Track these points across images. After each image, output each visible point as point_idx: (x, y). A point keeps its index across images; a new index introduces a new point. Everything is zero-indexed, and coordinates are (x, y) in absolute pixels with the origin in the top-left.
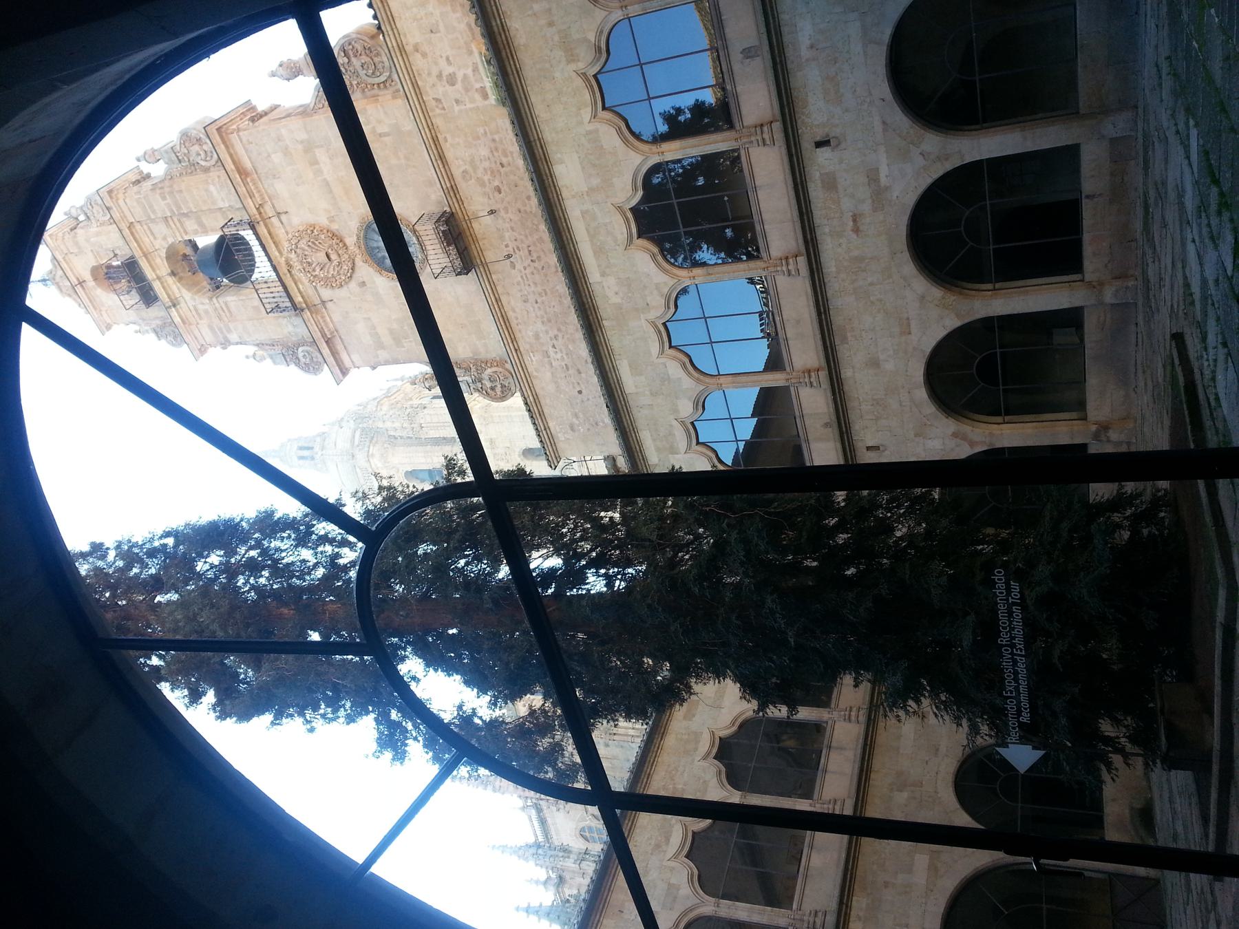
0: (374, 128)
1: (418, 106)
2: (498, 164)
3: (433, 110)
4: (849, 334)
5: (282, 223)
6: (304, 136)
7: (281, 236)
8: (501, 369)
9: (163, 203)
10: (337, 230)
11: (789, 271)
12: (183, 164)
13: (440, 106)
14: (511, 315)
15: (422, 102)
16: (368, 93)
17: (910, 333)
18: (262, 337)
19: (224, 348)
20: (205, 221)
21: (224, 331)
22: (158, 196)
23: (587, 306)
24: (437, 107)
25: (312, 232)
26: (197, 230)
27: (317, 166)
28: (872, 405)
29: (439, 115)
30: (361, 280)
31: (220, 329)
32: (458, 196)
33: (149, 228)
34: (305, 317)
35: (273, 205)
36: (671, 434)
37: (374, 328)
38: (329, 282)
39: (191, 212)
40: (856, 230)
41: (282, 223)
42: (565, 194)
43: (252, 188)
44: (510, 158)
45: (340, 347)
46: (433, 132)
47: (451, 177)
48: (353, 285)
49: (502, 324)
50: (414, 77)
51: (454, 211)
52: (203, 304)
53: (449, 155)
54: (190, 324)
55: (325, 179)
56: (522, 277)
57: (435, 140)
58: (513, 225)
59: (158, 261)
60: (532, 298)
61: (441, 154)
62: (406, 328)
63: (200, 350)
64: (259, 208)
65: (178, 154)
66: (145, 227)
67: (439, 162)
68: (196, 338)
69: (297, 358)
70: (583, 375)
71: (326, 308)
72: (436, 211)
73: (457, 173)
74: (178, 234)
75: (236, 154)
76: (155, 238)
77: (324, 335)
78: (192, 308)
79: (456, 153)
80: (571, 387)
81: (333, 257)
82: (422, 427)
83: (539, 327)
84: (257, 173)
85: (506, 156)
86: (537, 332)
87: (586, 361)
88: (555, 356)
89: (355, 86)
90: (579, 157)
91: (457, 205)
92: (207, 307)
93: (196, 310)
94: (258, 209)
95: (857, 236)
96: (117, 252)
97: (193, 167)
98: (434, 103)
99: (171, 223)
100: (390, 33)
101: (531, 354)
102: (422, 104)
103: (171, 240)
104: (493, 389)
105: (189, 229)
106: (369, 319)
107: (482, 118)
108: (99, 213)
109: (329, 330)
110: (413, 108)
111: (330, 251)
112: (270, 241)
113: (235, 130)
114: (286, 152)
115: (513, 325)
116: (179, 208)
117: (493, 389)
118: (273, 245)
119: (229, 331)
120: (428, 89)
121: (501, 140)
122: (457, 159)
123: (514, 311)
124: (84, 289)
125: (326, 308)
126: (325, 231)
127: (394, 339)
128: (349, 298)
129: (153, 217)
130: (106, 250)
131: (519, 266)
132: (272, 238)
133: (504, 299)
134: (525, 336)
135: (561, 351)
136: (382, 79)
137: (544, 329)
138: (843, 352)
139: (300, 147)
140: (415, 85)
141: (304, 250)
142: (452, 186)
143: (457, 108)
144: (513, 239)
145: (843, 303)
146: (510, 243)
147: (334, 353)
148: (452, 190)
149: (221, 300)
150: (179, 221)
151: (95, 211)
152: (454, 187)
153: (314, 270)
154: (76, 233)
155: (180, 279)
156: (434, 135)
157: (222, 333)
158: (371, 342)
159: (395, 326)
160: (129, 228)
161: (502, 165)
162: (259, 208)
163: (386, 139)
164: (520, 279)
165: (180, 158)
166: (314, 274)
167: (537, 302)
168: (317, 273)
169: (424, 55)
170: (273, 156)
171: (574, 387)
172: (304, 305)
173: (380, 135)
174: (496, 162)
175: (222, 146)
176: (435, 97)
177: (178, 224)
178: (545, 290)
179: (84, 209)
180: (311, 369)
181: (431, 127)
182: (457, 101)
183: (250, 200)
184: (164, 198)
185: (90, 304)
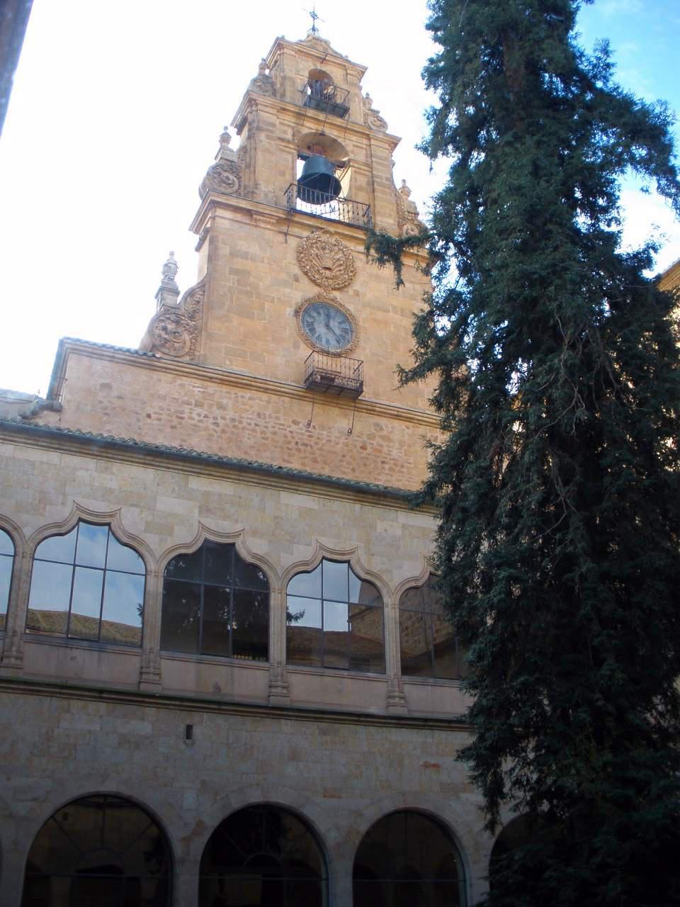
4: (329, 738)
8: (187, 350)
10: (347, 292)
11: (394, 697)
14: (248, 394)
17: (325, 796)
23: (382, 499)
25: (352, 272)
28: (246, 744)
36: (226, 517)
40: (426, 765)
44: (387, 472)
45: (239, 217)
46: (417, 422)
47: (381, 414)
48: (296, 270)
51: (357, 401)
53: (396, 423)
55: (389, 312)
56: (283, 425)
57: (409, 420)
58: (333, 444)
60: (261, 422)
62: (248, 288)
66: (364, 146)
68: (267, 106)
71: (280, 232)
73: (383, 421)
80: (157, 410)
83: (230, 414)
85: (390, 469)
87: (185, 441)
88: (195, 413)
91: (360, 406)
95: (422, 766)
99: (366, 168)
101: (200, 390)
109: (259, 220)
115: (240, 392)
121: (403, 472)
123: (250, 399)
124: (317, 57)
133: (265, 396)
135: (200, 421)
138: (312, 728)
144: (320, 436)
145: (363, 737)
148: (372, 410)
152: (372, 412)
155: (315, 134)
156: (414, 421)
159: (251, 279)
171: (156, 413)
174: (386, 458)
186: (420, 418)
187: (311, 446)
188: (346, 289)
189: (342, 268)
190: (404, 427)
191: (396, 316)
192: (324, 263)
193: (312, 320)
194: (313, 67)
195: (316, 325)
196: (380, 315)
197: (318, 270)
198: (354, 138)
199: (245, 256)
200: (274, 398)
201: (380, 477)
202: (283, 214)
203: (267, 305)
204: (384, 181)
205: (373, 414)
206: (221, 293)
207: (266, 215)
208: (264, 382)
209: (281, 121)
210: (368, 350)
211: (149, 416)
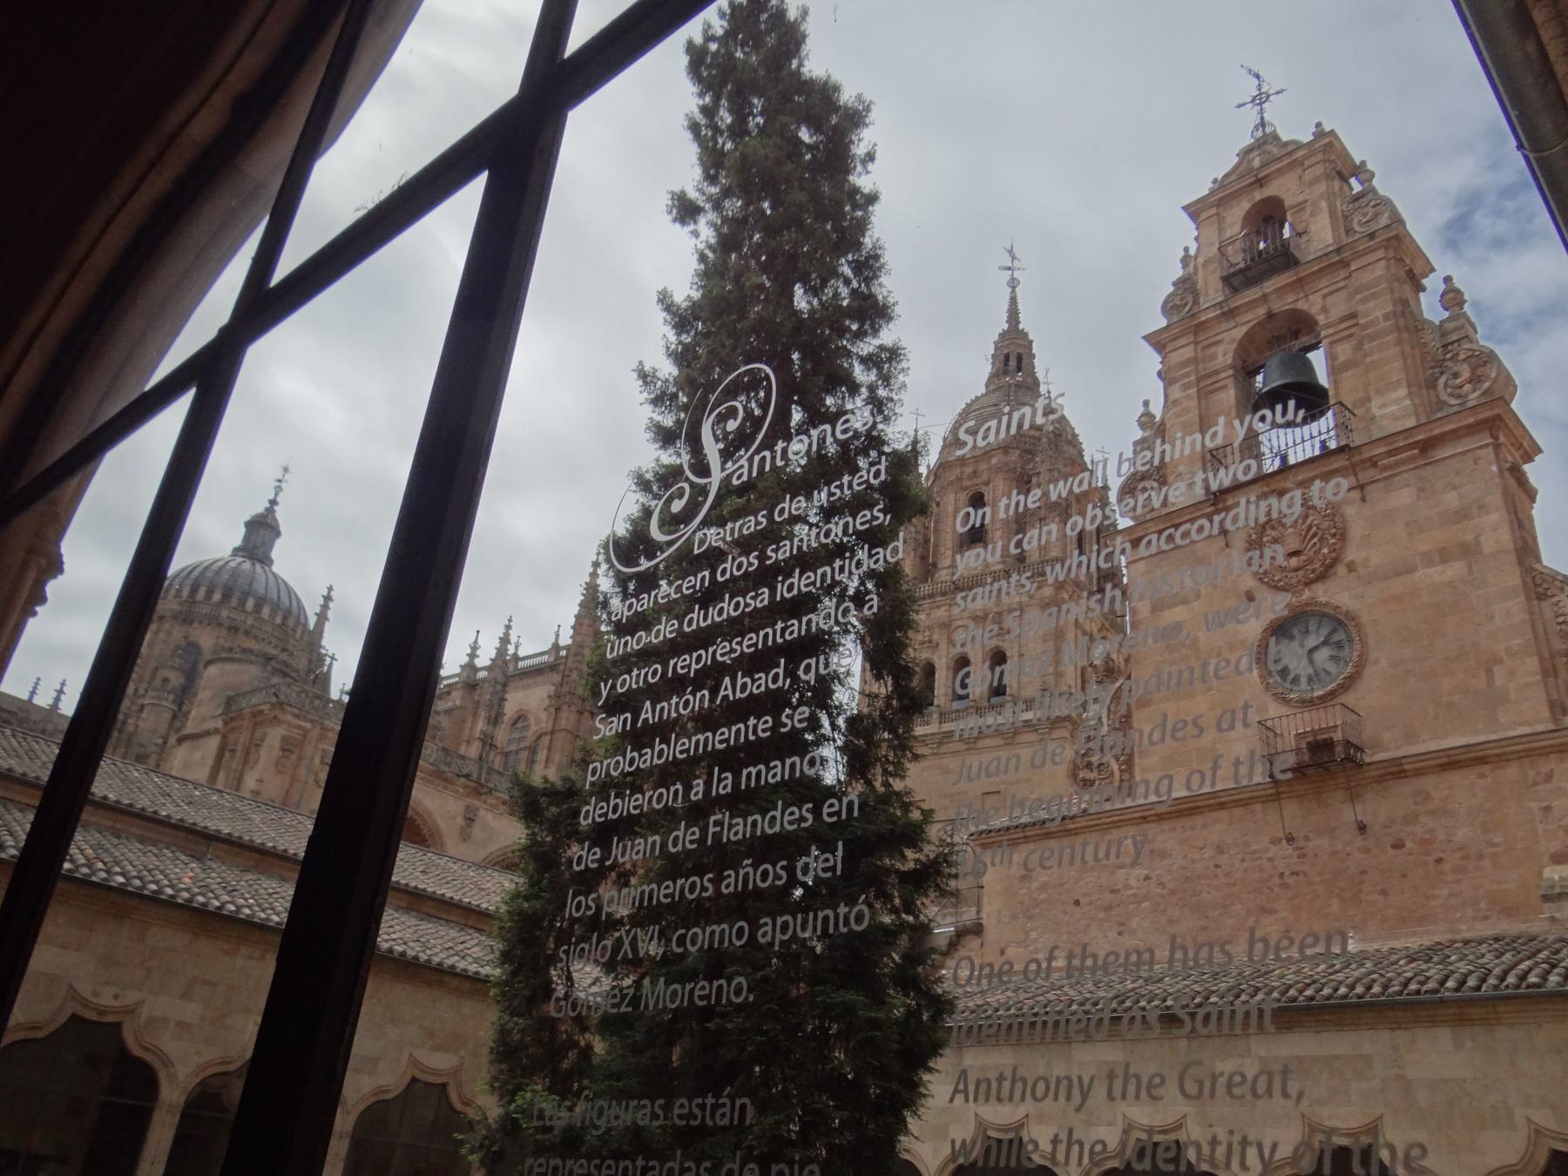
0: (1501, 662)
2: (1442, 855)
6: (1487, 547)
9: (1379, 314)
10: (1335, 574)
13: (1539, 779)
14: (1199, 820)
15: (1546, 752)
19: (1159, 374)
20: (1349, 373)
21: (1186, 381)
24: (1538, 773)
25: (1334, 535)
27: (1437, 560)
30: (1258, 596)
31: (1187, 375)
33: (1342, 288)
35: (1377, 481)
37: (1185, 602)
42: (1402, 1036)
43: (1404, 455)
47: (1419, 773)
52: (1225, 354)
53: (1455, 777)
54: (1196, 333)
55: (1416, 569)
56: (1255, 852)
57: (1483, 761)
63: (1159, 342)
64: (1373, 462)
65: (1456, 345)
66: (1342, 284)
67: (1445, 760)
70: (1102, 915)
73: (1428, 783)
74: (1331, 331)
76: (1324, 297)
78: (1219, 338)
79: (1462, 789)
81: (1294, 561)
82: (1041, 520)
86: (1170, 856)
90: (1465, 1081)
91: (1374, 773)
92: (1220, 359)
94: (1370, 459)
96: (1305, 237)
98: (1545, 769)
103: (1321, 319)
104: (1089, 766)
106: (1198, 597)
107: (1520, 845)
111: (1303, 557)
113: (1496, 438)
114: (1461, 515)
115: (1187, 822)
116: (1372, 338)
117: (1089, 766)
119: (1185, 387)
123: (1205, 826)
124: (1251, 184)
126: (1333, 555)
129: (1358, 297)
130: (1307, 226)
131: (1273, 848)
133: (1223, 814)
134: (1165, 837)
137: (1175, 867)
139: (1469, 537)
142: (1404, 771)
143: (1535, 805)
146: (1311, 844)
149: (1230, 382)
153: (1273, 528)
154: (1332, 179)
161: (1439, 861)
162: (1373, 462)
163: (1483, 675)
164: (1254, 847)
165: (1450, 347)
166: (1268, 527)
167: (1217, 866)
168: (1269, 531)
170: (1454, 494)
171: (1085, 895)
173: (1489, 671)
174: (1444, 851)
177: (1346, 333)
178: (1234, 884)
179: (1370, 196)
182: (1547, 809)
183: (1383, 450)
184: (1386, 317)
187: (1305, 874)
188: (1332, 571)
191: (1430, 571)
198: (1324, 283)
200: (1239, 812)
201: (1436, 892)
204: (1383, 324)
211: (1077, 903)
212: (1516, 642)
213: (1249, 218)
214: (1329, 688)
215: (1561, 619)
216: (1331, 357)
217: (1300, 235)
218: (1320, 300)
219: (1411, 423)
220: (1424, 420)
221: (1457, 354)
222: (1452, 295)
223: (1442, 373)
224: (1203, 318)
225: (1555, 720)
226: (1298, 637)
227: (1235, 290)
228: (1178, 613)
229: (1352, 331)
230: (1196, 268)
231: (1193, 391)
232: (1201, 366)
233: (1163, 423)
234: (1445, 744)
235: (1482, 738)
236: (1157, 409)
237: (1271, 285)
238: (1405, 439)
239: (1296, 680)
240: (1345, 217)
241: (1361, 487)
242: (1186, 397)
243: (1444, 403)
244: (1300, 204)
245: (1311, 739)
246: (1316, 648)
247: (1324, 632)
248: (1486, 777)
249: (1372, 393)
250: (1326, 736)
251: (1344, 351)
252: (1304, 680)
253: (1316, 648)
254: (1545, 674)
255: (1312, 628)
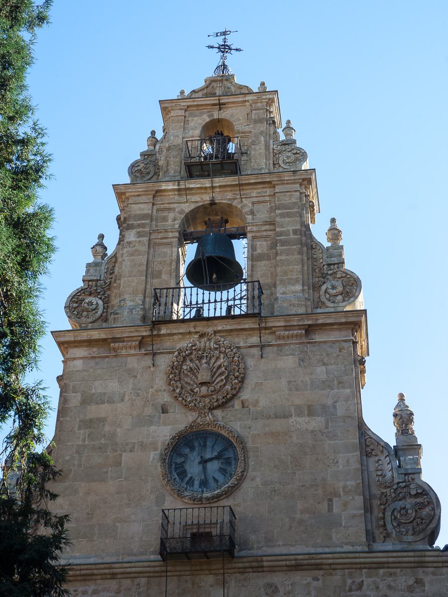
0: (340, 496)
1: (358, 560)
3: (351, 575)
5: (250, 347)
7: (236, 340)
9: (291, 228)
10: (233, 406)
12: (325, 267)
15: (361, 567)
16: (376, 502)
18: (125, 266)
20: (263, 263)
21: (140, 230)
22: (298, 227)
24: (353, 582)
25: (237, 378)
26: (256, 250)
27: (306, 412)
29: (344, 582)
31: (143, 226)
32: (250, 570)
34: (142, 329)
35: (271, 345)
37: (111, 401)
38: (175, 373)
39: (277, 254)
41: (250, 347)
43: (295, 332)
45: (95, 351)
46: (327, 567)
47: (273, 570)
48: (166, 398)
49: (83, 572)
50: (388, 568)
51: (235, 560)
52: (174, 220)
53: (299, 578)
55: (291, 416)
57: (318, 567)
59: (230, 195)
61: (301, 568)
62: (103, 441)
63: (124, 193)
65: (336, 266)
66: (267, 199)
67: (294, 562)
68: (139, 195)
69: (90, 295)
71: (145, 354)
72: (236, 535)
73: (277, 579)
74: (255, 229)
75: (332, 330)
77: (115, 340)
81: (204, 389)
84: (308, 343)
89: (384, 491)
91: (241, 565)
92: (170, 222)
93: (169, 209)
96: (244, 158)
97: (320, 275)
98: (358, 580)
99: (267, 227)
100: (440, 559)
102: (359, 566)
105: (258, 243)
106: (122, 400)
108: (288, 157)
110: (358, 555)
112: (233, 327)
116: (283, 243)
118: (228, 327)
119: (139, 235)
120: (373, 579)
122: (292, 584)
125: (145, 354)
127: (91, 420)
128: (152, 387)
129: (278, 212)
132: (236, 330)
133: (113, 584)
136: (389, 527)
139: (329, 402)
140: (380, 565)
141: (218, 358)
142: (262, 567)
147: (90, 343)
148: (258, 567)
150: (267, 237)
151: (289, 154)
152: (260, 569)
153: (191, 360)
156: (324, 566)
157: (139, 226)
158: (94, 391)
159: (107, 428)
160: (269, 182)
163: (326, 504)
165: (332, 267)
168: (188, 362)
169: (410, 589)
170: (323, 368)
172: (155, 333)
173: (330, 500)
175: (343, 320)
176: (365, 583)
177: (265, 233)
180: (75, 305)
181: (332, 568)
183: (282, 324)
184: (295, 232)
185: (196, 103)
186: (331, 561)
188: (230, 404)
189: (223, 377)
190: (309, 579)
191: (299, 419)
192: (199, 378)
193: (182, 459)
194: (208, 120)
195: (187, 467)
196: (277, 425)
197: (192, 390)
198: (254, 193)
199: (101, 399)
200: (127, 583)
202: (146, 331)
203: (126, 457)
204: (292, 236)
205: (263, 571)
206: (67, 458)
207: (126, 339)
208: (107, 566)
209: (158, 207)
210: (258, 480)
212: (351, 483)
213: (207, 127)
214: (216, 492)
215: (379, 473)
216: (252, 248)
217: (242, 153)
218: (250, 205)
219: (302, 310)
220: (310, 311)
221: (335, 273)
222: (337, 232)
223: (324, 283)
224: (163, 188)
225: (369, 545)
226: (197, 448)
227: (191, 176)
228: (103, 410)
229: (270, 233)
230: (160, 148)
231: (145, 239)
232: (154, 223)
233: (115, 256)
234: (293, 550)
235: (320, 550)
236: (111, 244)
237: (219, 181)
238: (299, 320)
239: (191, 482)
240: (275, 155)
241: (262, 347)
242: (139, 241)
243: (323, 303)
244: (246, 132)
245: (195, 531)
246: (211, 460)
247: (218, 449)
248: (318, 580)
249: (278, 282)
250: (208, 530)
251: (262, 246)
252: (197, 483)
253: (211, 460)
254: (366, 510)
255: (209, 444)
